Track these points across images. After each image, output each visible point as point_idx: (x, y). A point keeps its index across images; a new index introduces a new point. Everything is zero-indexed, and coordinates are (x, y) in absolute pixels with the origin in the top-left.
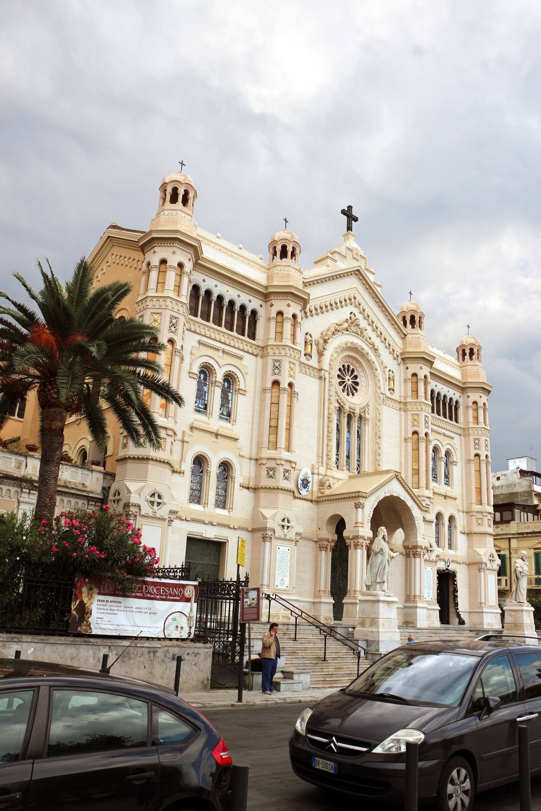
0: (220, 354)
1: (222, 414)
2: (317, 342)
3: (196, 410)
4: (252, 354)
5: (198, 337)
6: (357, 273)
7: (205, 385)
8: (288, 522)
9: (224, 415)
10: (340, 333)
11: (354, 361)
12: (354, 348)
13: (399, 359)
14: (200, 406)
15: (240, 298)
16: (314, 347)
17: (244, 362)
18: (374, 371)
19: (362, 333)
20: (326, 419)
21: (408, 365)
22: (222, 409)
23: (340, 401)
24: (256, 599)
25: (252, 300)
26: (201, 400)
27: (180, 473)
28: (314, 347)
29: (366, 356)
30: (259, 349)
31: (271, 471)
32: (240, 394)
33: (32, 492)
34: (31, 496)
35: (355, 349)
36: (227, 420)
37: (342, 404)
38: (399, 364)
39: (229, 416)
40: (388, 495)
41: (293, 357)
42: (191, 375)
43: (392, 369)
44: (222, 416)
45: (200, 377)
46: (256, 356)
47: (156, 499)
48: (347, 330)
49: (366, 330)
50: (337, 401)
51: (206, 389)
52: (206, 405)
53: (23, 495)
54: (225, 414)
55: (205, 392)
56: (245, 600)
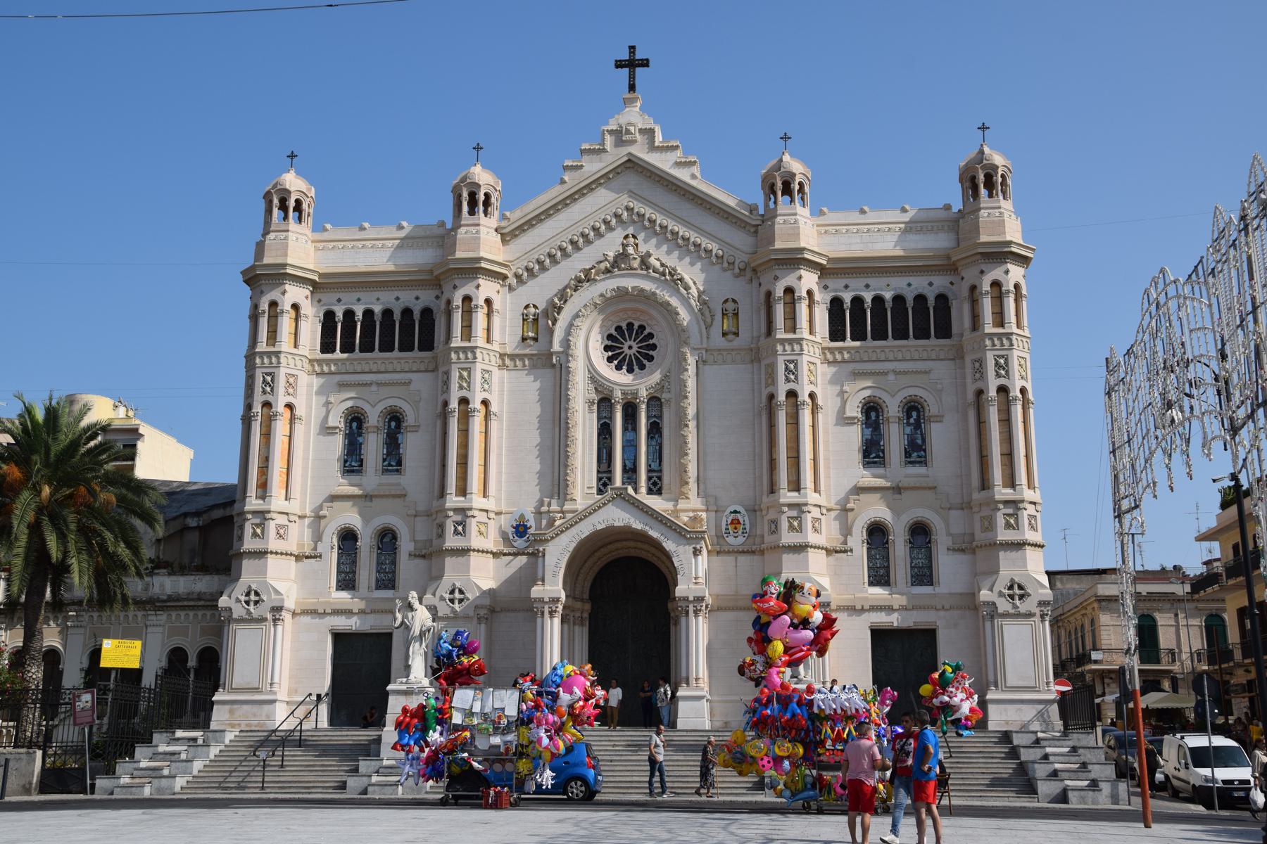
1: (390, 465)
3: (348, 471)
4: (426, 371)
6: (628, 165)
7: (360, 436)
8: (461, 592)
9: (392, 466)
11: (639, 314)
13: (749, 273)
14: (353, 464)
15: (400, 301)
17: (412, 387)
22: (388, 459)
24: (90, 702)
25: (419, 295)
26: (354, 457)
27: (315, 557)
31: (459, 525)
33: (158, 613)
34: (159, 617)
35: (621, 294)
36: (397, 470)
39: (401, 465)
40: (600, 527)
43: (730, 296)
44: (390, 468)
45: (351, 427)
47: (253, 597)
49: (649, 255)
51: (360, 439)
52: (362, 461)
53: (150, 618)
54: (393, 463)
55: (361, 444)
56: (77, 704)
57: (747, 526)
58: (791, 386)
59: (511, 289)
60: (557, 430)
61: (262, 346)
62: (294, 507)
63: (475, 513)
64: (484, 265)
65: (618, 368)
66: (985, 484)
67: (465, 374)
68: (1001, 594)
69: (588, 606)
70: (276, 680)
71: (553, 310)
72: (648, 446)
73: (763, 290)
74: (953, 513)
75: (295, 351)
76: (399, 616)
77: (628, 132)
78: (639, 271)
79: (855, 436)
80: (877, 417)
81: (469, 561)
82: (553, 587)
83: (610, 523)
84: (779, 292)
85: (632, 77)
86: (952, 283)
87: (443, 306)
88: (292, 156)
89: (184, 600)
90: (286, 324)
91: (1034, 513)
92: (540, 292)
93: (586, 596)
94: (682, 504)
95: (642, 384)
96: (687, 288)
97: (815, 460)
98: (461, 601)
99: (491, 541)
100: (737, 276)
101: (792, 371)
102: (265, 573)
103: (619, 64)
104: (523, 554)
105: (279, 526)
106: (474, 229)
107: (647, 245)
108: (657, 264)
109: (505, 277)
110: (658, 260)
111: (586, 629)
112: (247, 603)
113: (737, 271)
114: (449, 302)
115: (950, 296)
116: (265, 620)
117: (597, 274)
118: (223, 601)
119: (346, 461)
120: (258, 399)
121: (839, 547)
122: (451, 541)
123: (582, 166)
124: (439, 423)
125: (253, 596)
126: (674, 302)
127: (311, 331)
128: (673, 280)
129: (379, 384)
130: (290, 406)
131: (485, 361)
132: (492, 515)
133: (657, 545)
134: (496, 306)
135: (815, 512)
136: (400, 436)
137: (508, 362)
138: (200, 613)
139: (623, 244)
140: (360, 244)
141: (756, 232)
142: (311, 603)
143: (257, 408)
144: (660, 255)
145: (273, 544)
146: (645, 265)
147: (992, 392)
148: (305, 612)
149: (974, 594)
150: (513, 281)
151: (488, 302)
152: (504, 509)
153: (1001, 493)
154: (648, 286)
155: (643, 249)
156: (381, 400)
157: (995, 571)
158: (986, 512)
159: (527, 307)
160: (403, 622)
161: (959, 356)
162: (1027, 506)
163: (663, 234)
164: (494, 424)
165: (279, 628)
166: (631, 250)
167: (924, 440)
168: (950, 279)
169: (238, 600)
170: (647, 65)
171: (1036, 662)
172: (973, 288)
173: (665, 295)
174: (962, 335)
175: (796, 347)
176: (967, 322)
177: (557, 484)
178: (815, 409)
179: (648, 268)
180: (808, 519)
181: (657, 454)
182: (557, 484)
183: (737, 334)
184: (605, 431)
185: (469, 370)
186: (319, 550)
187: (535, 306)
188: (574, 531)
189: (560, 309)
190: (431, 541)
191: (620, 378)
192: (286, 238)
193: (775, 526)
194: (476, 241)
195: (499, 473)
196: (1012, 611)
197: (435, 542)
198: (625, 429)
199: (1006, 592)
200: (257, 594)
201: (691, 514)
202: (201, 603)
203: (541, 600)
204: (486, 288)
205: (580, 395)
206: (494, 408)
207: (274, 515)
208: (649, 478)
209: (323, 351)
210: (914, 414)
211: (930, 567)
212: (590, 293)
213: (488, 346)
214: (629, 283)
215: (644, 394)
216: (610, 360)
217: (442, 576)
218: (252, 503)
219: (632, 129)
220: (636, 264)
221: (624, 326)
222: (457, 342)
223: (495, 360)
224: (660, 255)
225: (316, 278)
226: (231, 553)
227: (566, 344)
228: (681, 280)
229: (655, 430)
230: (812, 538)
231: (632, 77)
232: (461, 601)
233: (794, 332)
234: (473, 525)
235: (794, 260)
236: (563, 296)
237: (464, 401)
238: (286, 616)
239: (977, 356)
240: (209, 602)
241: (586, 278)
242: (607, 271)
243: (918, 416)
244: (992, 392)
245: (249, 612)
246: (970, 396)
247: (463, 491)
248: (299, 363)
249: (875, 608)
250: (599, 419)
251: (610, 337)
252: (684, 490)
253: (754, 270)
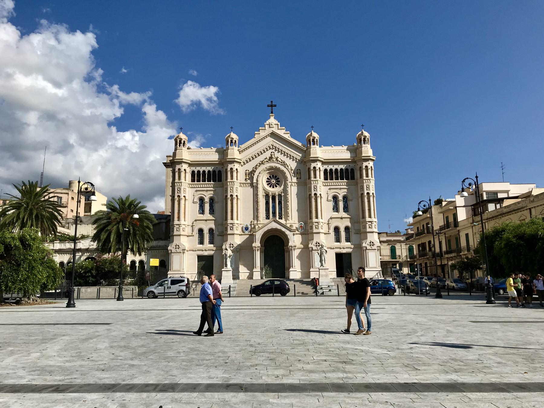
1: (211, 212)
35: (271, 168)
47: (177, 247)
49: (278, 158)
52: (203, 211)
57: (304, 227)
58: (315, 192)
59: (242, 166)
61: (177, 180)
62: (186, 223)
63: (235, 224)
64: (236, 160)
65: (270, 187)
66: (364, 217)
67: (232, 188)
68: (368, 244)
69: (264, 248)
70: (184, 268)
71: (253, 172)
72: (279, 207)
73: (307, 167)
74: (356, 224)
75: (185, 182)
76: (224, 252)
77: (272, 125)
78: (275, 162)
79: (331, 204)
80: (336, 199)
81: (234, 237)
82: (257, 244)
83: (272, 228)
84: (312, 168)
85: (272, 109)
87: (224, 170)
88: (181, 129)
89: (155, 247)
90: (183, 174)
91: (376, 224)
92: (250, 167)
93: (263, 245)
94: (288, 222)
95: (277, 190)
96: (288, 166)
97: (321, 211)
98: (232, 247)
99: (239, 231)
100: (301, 163)
101: (315, 188)
102: (180, 240)
103: (268, 106)
104: (247, 235)
105: (183, 228)
106: (232, 150)
107: (277, 154)
108: (280, 160)
109: (240, 163)
111: (263, 254)
112: (176, 248)
113: (300, 162)
114: (226, 169)
115: (354, 169)
116: (181, 252)
117: (265, 162)
118: (169, 248)
119: (199, 211)
120: (176, 195)
121: (327, 232)
122: (229, 232)
123: (260, 134)
124: (224, 201)
125: (178, 247)
126: (285, 170)
127: (189, 176)
128: (284, 164)
130: (184, 196)
131: (237, 185)
132: (239, 225)
133: (283, 233)
134: (238, 170)
135: (322, 224)
136: (213, 204)
137: (242, 185)
138: (160, 251)
139: (271, 155)
140: (201, 153)
141: (305, 152)
142: (191, 248)
143: (176, 197)
144: (281, 157)
145: (182, 233)
147: (366, 194)
148: (190, 250)
149: (361, 245)
150: (242, 164)
151: (237, 169)
152: (242, 223)
153: (368, 219)
154: (278, 166)
155: (276, 156)
157: (367, 239)
158: (364, 224)
159: (246, 171)
160: (225, 253)
161: (357, 184)
162: (374, 222)
163: (281, 152)
164: (239, 201)
165: (184, 255)
166: (273, 156)
167: (348, 206)
168: (355, 164)
169: (173, 248)
170: (276, 106)
171: (376, 261)
172: (360, 167)
173: (282, 168)
174: (357, 179)
175: (317, 182)
176: (359, 176)
177: (256, 217)
178: (321, 197)
179: (278, 161)
180: (320, 226)
181: (280, 209)
182: (256, 217)
183: (300, 178)
184: (267, 203)
185: (233, 188)
186: (193, 234)
187: (248, 171)
188: (263, 229)
189: (255, 171)
190: (223, 232)
191: (271, 190)
192: (182, 151)
193: (311, 228)
194: (233, 154)
195: (240, 214)
196: (371, 249)
197: (224, 232)
198: (272, 202)
199: (369, 244)
200: (178, 246)
201: (290, 224)
202: (161, 248)
203: (255, 247)
204: (236, 166)
205: (261, 194)
206: (239, 197)
207: (182, 225)
208: (279, 215)
209: (192, 182)
210: (345, 199)
211: (350, 238)
212: (263, 167)
213: (237, 181)
214: (273, 165)
215: (277, 194)
216: (268, 184)
217: (227, 241)
218: (176, 222)
219: (273, 124)
220: (275, 160)
222: (229, 180)
223: (239, 185)
224: (281, 157)
225: (189, 162)
226: (170, 235)
227: (257, 180)
228: (286, 164)
229: (280, 203)
230: (321, 231)
231: (272, 109)
232: (232, 247)
233: (316, 178)
234: (235, 227)
235: (315, 160)
236: (256, 168)
237: (232, 196)
238: (186, 251)
239: (361, 185)
240: (165, 248)
241: (262, 163)
242: (267, 161)
243: (346, 199)
244: (366, 194)
245: (176, 251)
246: (360, 195)
247: (232, 219)
248: (186, 185)
249: (336, 248)
250: (265, 200)
251: (268, 179)
252: (288, 218)
253: (305, 162)
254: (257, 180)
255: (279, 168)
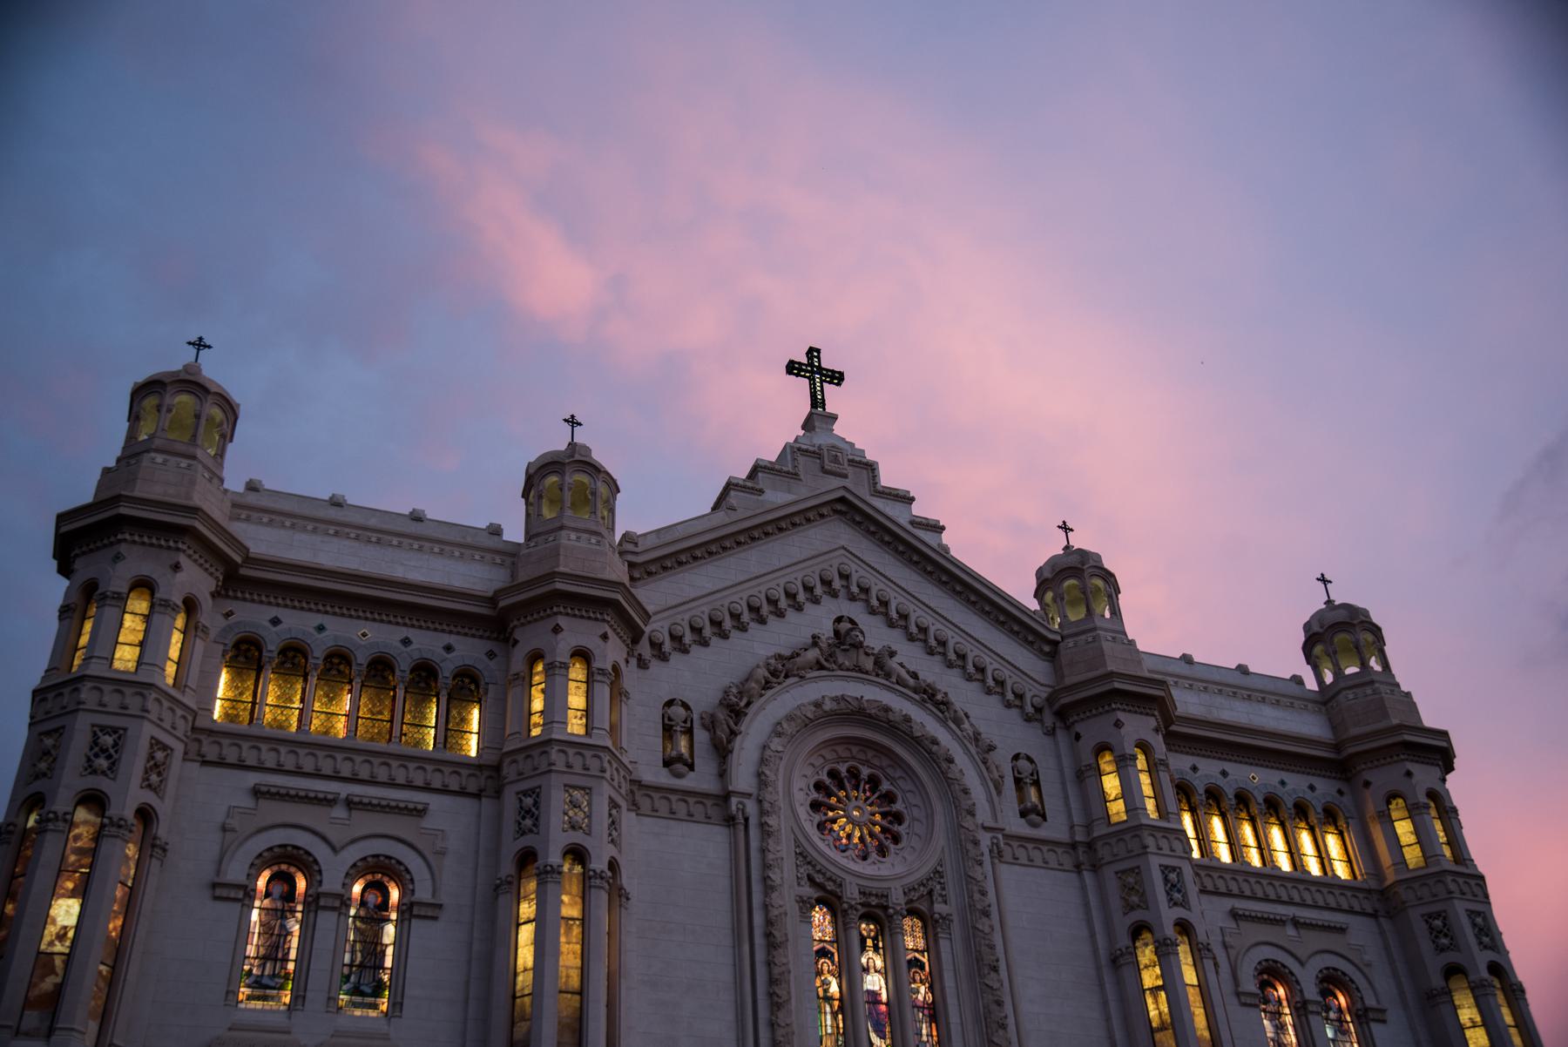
0: (339, 812)
2: (707, 721)
4: (462, 793)
5: (253, 779)
6: (839, 507)
10: (791, 680)
11: (870, 754)
12: (853, 713)
13: (1049, 719)
15: (413, 647)
16: (701, 736)
17: (427, 822)
18: (944, 765)
19: (879, 663)
20: (759, 940)
21: (1078, 728)
23: (819, 878)
28: (701, 736)
29: (904, 727)
30: (486, 773)
32: (419, 917)
35: (856, 713)
37: (830, 886)
38: (1051, 733)
41: (578, 768)
42: (219, 892)
43: (1023, 751)
46: (477, 796)
48: (822, 668)
49: (892, 654)
50: (810, 879)
54: (368, 990)
60: (746, 948)
71: (735, 709)
86: (1340, 792)
107: (876, 635)
110: (901, 665)
129: (351, 804)
146: (882, 668)
156: (353, 841)
159: (670, 703)
220: (868, 664)
221: (843, 769)
254: (762, 780)
255: (907, 719)
